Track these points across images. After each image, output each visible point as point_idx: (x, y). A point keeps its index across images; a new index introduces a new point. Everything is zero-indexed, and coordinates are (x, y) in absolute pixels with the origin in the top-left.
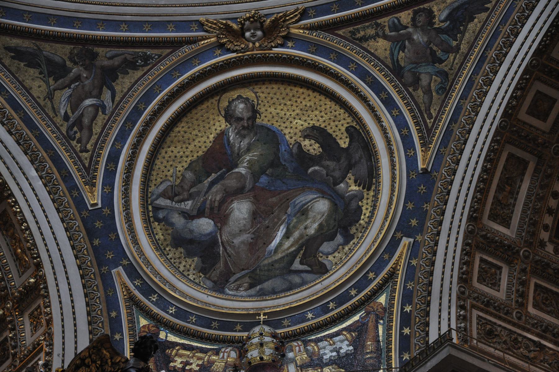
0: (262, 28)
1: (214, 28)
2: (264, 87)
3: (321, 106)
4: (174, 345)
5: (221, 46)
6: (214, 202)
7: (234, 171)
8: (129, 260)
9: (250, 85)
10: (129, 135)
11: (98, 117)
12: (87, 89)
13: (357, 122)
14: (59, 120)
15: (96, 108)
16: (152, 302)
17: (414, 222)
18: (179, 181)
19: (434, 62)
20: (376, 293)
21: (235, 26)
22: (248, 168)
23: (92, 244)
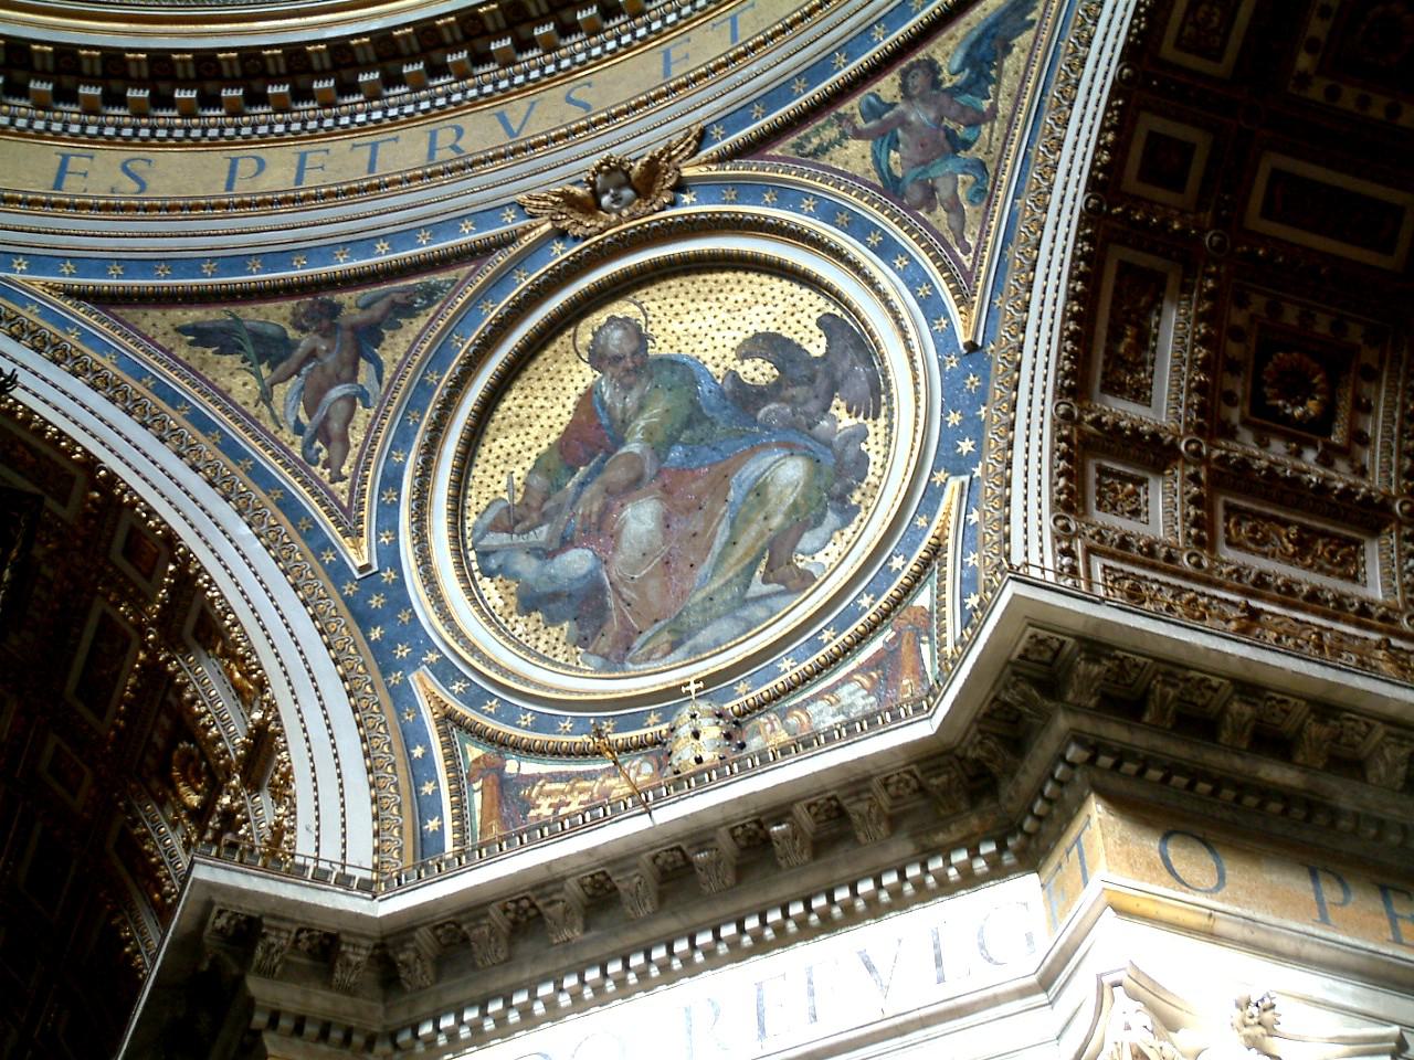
0: (628, 183)
1: (544, 208)
2: (653, 290)
3: (763, 295)
4: (533, 780)
5: (562, 235)
6: (590, 516)
7: (619, 453)
8: (440, 652)
9: (628, 294)
10: (416, 433)
11: (356, 415)
12: (330, 370)
13: (835, 303)
14: (286, 436)
15: (351, 401)
16: (489, 715)
17: (966, 446)
18: (519, 497)
19: (955, 151)
20: (908, 591)
21: (579, 191)
22: (649, 441)
23: (368, 639)
